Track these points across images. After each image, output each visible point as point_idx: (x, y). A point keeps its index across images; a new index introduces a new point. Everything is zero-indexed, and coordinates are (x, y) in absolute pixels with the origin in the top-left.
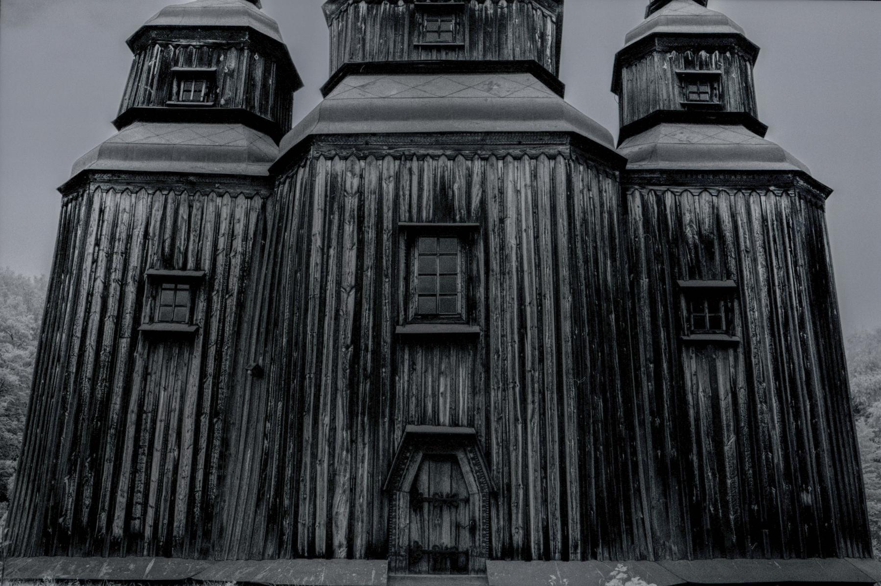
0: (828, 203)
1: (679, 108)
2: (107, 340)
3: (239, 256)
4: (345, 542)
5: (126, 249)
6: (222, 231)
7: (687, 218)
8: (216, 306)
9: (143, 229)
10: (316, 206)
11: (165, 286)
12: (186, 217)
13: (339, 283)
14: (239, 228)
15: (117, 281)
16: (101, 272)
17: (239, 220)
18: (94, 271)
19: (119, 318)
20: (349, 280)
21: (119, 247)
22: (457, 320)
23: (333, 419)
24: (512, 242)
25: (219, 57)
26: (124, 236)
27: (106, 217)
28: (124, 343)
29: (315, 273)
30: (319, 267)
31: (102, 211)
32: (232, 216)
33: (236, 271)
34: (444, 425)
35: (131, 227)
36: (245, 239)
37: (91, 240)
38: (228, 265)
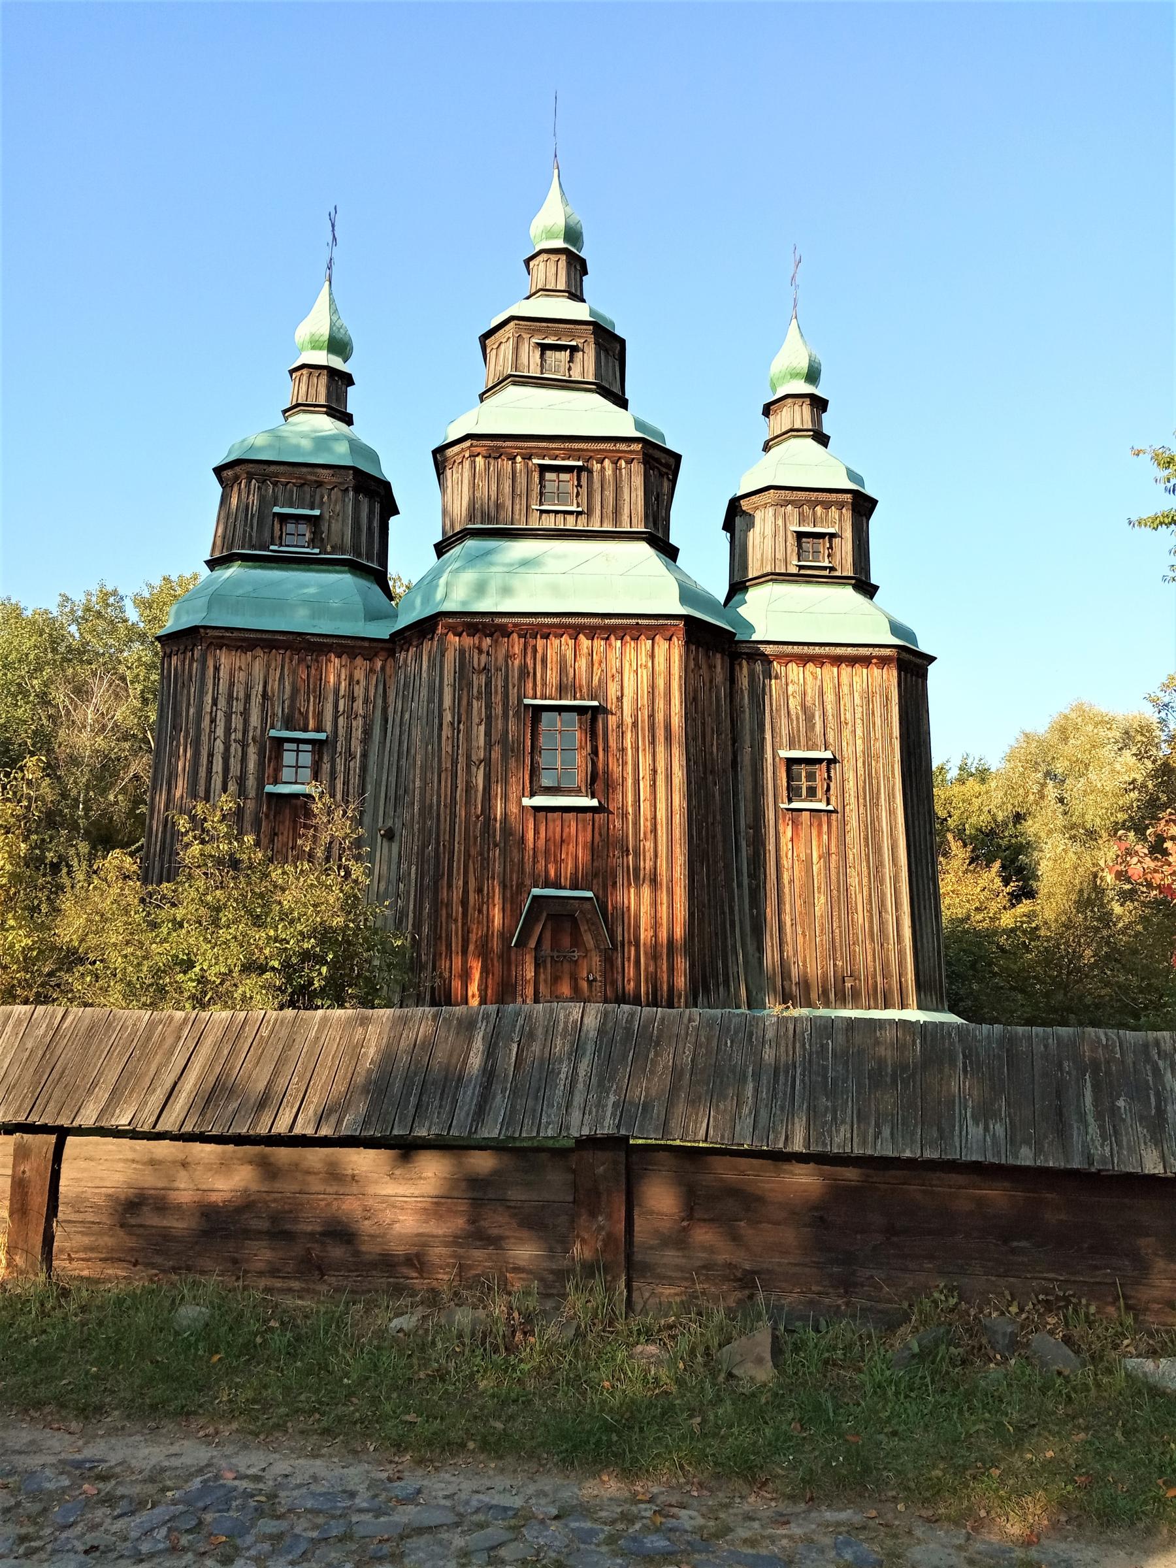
0: (932, 669)
3: (360, 721)
4: (477, 993)
5: (245, 709)
6: (342, 693)
8: (340, 767)
9: (261, 689)
10: (446, 682)
11: (287, 746)
12: (304, 677)
13: (469, 757)
14: (359, 691)
15: (235, 741)
16: (220, 731)
17: (358, 682)
21: (238, 706)
23: (466, 883)
25: (322, 497)
26: (242, 695)
27: (221, 675)
29: (447, 747)
30: (450, 742)
32: (351, 677)
33: (358, 734)
34: (565, 888)
35: (248, 688)
36: (366, 701)
37: (208, 699)
38: (349, 729)
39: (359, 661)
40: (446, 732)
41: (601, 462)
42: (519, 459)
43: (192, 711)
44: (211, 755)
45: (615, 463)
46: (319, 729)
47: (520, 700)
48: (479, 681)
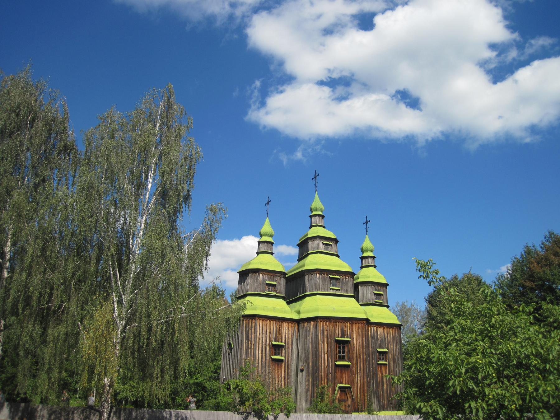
1: (374, 303)
2: (264, 360)
7: (379, 333)
13: (324, 352)
14: (290, 332)
16: (261, 342)
18: (259, 342)
19: (266, 354)
20: (326, 350)
21: (264, 335)
22: (345, 361)
24: (355, 343)
28: (267, 361)
31: (259, 326)
32: (288, 329)
33: (290, 343)
39: (290, 324)
40: (320, 346)
41: (343, 277)
42: (326, 275)
43: (253, 336)
44: (259, 348)
45: (346, 277)
46: (282, 342)
47: (334, 338)
48: (325, 333)
